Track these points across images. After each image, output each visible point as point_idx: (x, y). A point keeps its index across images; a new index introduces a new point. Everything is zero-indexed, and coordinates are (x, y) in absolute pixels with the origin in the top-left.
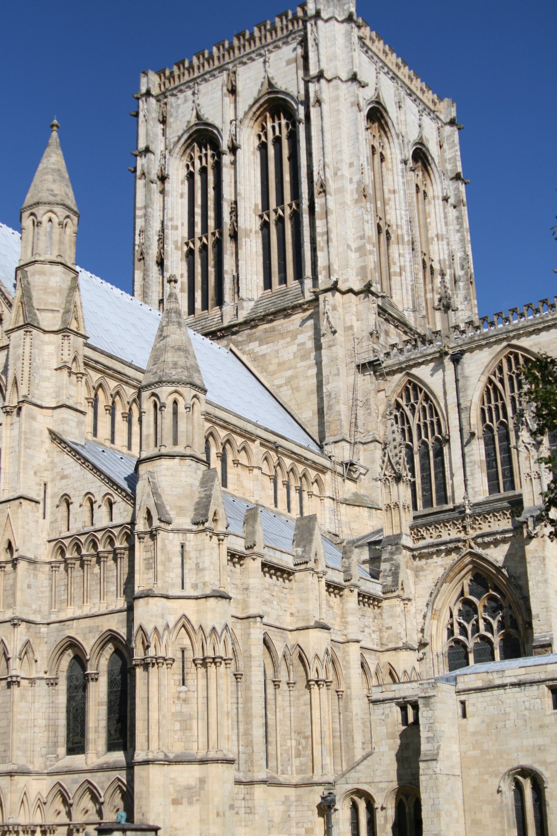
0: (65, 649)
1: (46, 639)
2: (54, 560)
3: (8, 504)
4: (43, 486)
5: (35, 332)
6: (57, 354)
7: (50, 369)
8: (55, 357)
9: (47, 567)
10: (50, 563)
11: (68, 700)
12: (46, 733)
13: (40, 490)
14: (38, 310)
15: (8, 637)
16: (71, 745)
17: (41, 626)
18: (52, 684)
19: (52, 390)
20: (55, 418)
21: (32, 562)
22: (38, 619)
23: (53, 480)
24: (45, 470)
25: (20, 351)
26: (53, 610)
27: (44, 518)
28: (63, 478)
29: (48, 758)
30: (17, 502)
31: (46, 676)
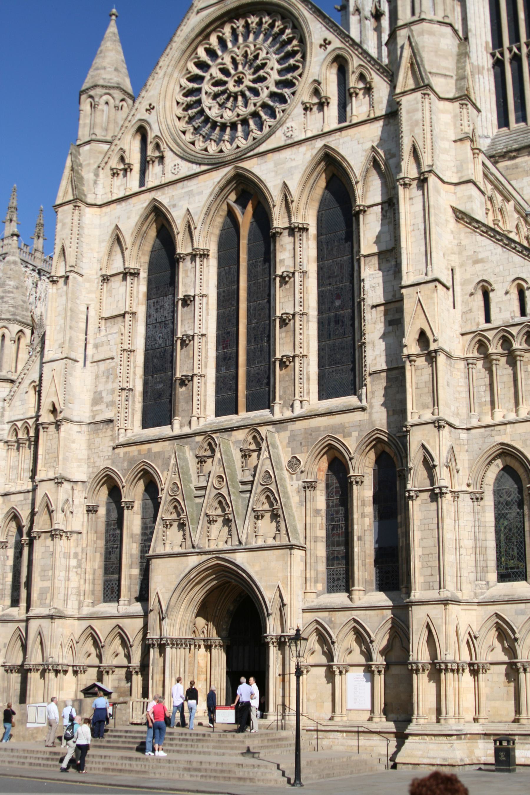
0: (494, 459)
1: (466, 447)
2: (471, 355)
3: (418, 288)
4: (450, 272)
5: (432, 96)
6: (455, 125)
7: (448, 140)
8: (452, 128)
9: (462, 364)
10: (466, 359)
11: (496, 518)
12: (473, 556)
13: (448, 274)
14: (430, 73)
15: (431, 441)
16: (504, 571)
17: (460, 430)
18: (477, 499)
19: (452, 164)
20: (459, 195)
21: (449, 356)
22: (457, 424)
23: (462, 265)
24: (452, 253)
25: (418, 116)
26: (473, 413)
27: (454, 308)
28: (476, 262)
29: (476, 585)
30: (432, 285)
31: (470, 489)
